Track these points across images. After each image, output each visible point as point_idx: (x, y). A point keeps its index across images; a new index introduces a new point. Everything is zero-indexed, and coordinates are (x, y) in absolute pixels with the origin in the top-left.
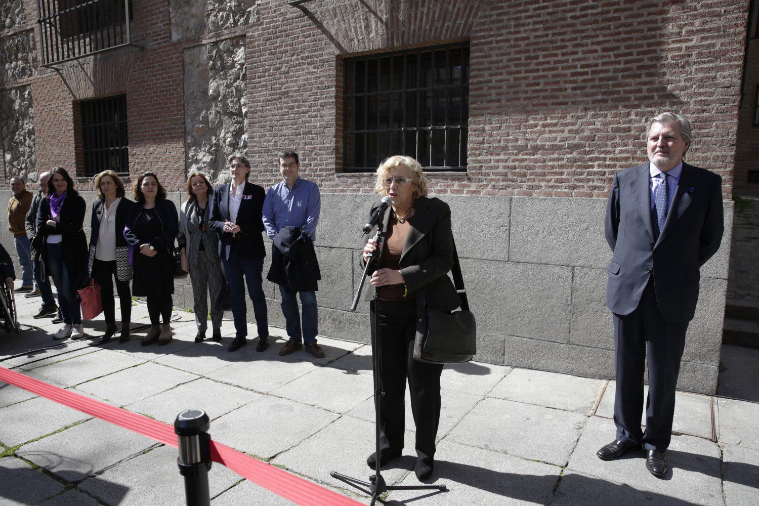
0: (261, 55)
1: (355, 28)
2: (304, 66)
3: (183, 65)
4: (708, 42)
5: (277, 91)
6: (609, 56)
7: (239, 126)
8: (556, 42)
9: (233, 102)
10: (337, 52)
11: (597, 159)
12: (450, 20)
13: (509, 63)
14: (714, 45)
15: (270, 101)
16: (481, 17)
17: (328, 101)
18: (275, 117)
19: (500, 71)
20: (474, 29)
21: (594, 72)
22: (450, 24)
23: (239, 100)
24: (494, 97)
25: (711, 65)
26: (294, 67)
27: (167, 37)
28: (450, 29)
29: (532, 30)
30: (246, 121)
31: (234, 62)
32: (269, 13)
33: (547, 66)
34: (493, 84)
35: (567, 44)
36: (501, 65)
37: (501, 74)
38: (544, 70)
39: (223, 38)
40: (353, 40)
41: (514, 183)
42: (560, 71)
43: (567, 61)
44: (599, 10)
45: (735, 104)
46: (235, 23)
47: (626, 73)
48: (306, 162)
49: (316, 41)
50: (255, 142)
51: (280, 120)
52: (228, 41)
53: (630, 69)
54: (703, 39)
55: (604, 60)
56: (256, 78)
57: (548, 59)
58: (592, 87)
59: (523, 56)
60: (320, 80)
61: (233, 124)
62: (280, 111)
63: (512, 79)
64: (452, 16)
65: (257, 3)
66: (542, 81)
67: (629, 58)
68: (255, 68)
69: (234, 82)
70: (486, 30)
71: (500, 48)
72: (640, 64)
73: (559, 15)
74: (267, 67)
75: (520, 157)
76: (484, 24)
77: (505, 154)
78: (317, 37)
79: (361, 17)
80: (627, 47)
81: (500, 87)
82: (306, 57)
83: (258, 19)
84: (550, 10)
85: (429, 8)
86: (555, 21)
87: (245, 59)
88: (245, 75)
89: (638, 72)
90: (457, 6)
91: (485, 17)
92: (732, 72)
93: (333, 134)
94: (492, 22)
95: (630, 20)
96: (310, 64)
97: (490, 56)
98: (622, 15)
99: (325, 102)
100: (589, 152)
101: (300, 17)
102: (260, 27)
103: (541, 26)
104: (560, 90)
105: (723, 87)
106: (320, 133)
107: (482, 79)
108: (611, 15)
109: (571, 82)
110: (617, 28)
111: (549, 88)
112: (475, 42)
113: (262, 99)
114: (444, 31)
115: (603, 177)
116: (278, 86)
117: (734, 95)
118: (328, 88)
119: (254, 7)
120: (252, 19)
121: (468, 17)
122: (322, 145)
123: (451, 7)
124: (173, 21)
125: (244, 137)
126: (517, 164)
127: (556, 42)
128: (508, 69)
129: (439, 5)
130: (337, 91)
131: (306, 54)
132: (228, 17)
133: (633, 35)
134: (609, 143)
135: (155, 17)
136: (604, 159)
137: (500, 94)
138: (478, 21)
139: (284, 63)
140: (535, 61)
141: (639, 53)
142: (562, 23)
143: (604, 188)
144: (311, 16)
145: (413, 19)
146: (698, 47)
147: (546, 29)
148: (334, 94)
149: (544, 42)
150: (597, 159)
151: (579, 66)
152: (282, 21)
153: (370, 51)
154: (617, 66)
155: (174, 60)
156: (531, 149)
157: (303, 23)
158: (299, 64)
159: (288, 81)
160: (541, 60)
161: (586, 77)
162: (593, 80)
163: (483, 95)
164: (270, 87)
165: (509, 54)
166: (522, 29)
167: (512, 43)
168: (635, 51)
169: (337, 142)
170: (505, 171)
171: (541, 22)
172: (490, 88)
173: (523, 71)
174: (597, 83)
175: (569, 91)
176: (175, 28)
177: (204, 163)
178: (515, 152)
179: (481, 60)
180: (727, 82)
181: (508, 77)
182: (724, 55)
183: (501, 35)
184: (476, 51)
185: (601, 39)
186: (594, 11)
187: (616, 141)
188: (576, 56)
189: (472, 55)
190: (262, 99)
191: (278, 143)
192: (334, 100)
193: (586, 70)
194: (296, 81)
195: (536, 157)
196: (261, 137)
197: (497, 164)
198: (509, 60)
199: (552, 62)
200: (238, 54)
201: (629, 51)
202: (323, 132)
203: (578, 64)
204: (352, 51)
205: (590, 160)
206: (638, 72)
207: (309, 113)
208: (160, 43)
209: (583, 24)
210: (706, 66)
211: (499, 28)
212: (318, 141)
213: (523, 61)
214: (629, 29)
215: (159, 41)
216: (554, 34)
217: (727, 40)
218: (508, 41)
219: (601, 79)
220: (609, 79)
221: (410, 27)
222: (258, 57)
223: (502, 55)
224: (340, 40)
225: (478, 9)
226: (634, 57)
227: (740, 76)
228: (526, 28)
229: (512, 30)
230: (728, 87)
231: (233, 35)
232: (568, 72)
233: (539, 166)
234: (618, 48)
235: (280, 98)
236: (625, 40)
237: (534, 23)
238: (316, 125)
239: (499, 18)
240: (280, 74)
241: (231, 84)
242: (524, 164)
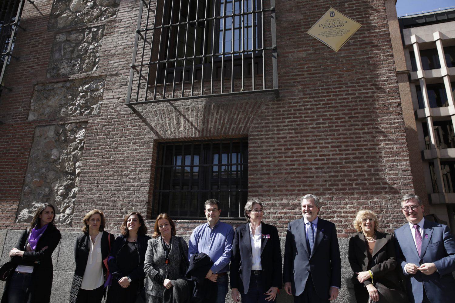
0: (98, 135)
1: (170, 124)
2: (129, 145)
3: (33, 137)
4: (390, 146)
5: (107, 160)
6: (336, 151)
7: (71, 182)
8: (303, 141)
9: (69, 165)
10: (155, 137)
11: (335, 212)
12: (235, 124)
13: (274, 152)
14: (393, 148)
15: (100, 166)
16: (255, 124)
17: (145, 168)
18: (103, 177)
19: (268, 156)
20: (250, 130)
21: (328, 159)
22: (235, 126)
23: (75, 164)
24: (265, 171)
25: (393, 158)
26: (122, 144)
27: (25, 117)
28: (235, 129)
29: (288, 133)
30: (77, 179)
31: (75, 138)
32: (108, 109)
33: (299, 154)
34: (264, 163)
35: (310, 142)
36: (269, 152)
37: (269, 158)
38: (297, 157)
39: (70, 122)
40: (167, 131)
41: (281, 228)
42: (307, 158)
43: (311, 152)
44: (327, 125)
45: (411, 180)
46: (81, 114)
47: (347, 161)
48: (124, 210)
49: (140, 129)
50: (83, 194)
51: (105, 180)
52: (73, 124)
53: (349, 158)
54: (386, 144)
55: (333, 153)
56: (91, 150)
57: (299, 150)
58: (328, 168)
59: (283, 148)
60: (141, 154)
61: (66, 180)
62: (107, 173)
63: (276, 161)
64: (236, 122)
65: (99, 103)
66: (296, 163)
67: (347, 152)
68: (92, 143)
69: (72, 152)
70: (259, 131)
71: (268, 142)
72: (355, 156)
73: (304, 126)
74: (101, 143)
75: (285, 211)
76: (258, 127)
77: (274, 209)
78: (142, 127)
79: (174, 117)
80: (346, 146)
81: (269, 166)
82: (132, 139)
83: (99, 113)
84: (298, 123)
85: (221, 116)
86: (302, 129)
87: (85, 137)
88: (82, 147)
89: (354, 160)
90: (239, 116)
91: (258, 124)
92: (405, 163)
93: (147, 192)
94: (263, 127)
95: (345, 132)
96: (134, 143)
97: (262, 146)
98: (341, 129)
99: (143, 169)
100: (330, 208)
101: (130, 114)
102: (100, 118)
103: (294, 131)
104: (308, 169)
105: (402, 171)
106: (136, 190)
107: (257, 160)
108: (334, 128)
109: (314, 164)
110: (339, 135)
111: (301, 167)
112: (251, 138)
113: (93, 164)
114: (231, 130)
115: (341, 224)
116: (107, 156)
117: (409, 176)
118: (146, 160)
119: (97, 105)
120: (94, 112)
121: (247, 123)
122: (137, 199)
123: (235, 117)
124: (32, 108)
125: (75, 190)
126: (282, 215)
127: (303, 141)
128: (274, 155)
129: (227, 115)
130: (152, 163)
131: (132, 137)
132: (76, 110)
133: (348, 140)
134: (342, 202)
135: (18, 104)
136: (340, 212)
137: (270, 170)
138: (254, 126)
139: (115, 141)
140: (291, 151)
141: (353, 150)
142: (306, 130)
143: (342, 231)
144: (138, 114)
145: (210, 121)
146: (385, 148)
147: (296, 133)
148: (150, 164)
149: (296, 141)
150: (335, 212)
151: (318, 155)
152: (117, 115)
153: (179, 139)
154: (341, 157)
155: (27, 133)
156: (291, 206)
157: (132, 118)
158: (126, 143)
159: (115, 154)
160: (294, 150)
161: (323, 162)
162: (328, 164)
163: (258, 170)
164: (101, 156)
165: (274, 146)
166: (282, 132)
167: (276, 140)
168: (350, 148)
169: (149, 197)
170: (275, 220)
171: (293, 129)
172: (262, 166)
173: (284, 156)
174: (330, 165)
175: (314, 170)
176: (33, 112)
177: (35, 208)
178: (281, 207)
179: (255, 149)
180: (404, 168)
181: (274, 160)
182: (399, 154)
183: (269, 135)
184: (253, 143)
185: (330, 141)
186: (324, 125)
187: (346, 201)
188: (316, 150)
189: (249, 145)
190: (93, 164)
191: (102, 196)
192: (150, 168)
193: (323, 157)
194: (122, 154)
195: (295, 211)
196: (88, 191)
197: (268, 215)
198: (274, 150)
199: (302, 152)
200: (79, 133)
201: (347, 148)
202: (140, 190)
203: (318, 154)
204: (166, 138)
205: (331, 213)
206: (354, 160)
207: (130, 176)
208: (18, 121)
209: (318, 132)
210: (391, 159)
211: (267, 131)
212: (134, 196)
213: (283, 151)
214: (345, 136)
215: (17, 119)
216: (301, 136)
217: (399, 146)
218: (273, 138)
219: (333, 163)
220: (338, 163)
221: (208, 126)
222: (95, 136)
223: (270, 146)
224: (158, 129)
225: (253, 119)
226: (350, 152)
227: (410, 165)
228: (284, 132)
229: (275, 132)
230: (405, 171)
231: (78, 121)
232: (313, 158)
233: (298, 217)
234: (341, 146)
235: (108, 165)
236: (344, 142)
237: (289, 129)
238: (135, 185)
239: (266, 125)
240: (110, 148)
241: (70, 153)
242: (287, 215)
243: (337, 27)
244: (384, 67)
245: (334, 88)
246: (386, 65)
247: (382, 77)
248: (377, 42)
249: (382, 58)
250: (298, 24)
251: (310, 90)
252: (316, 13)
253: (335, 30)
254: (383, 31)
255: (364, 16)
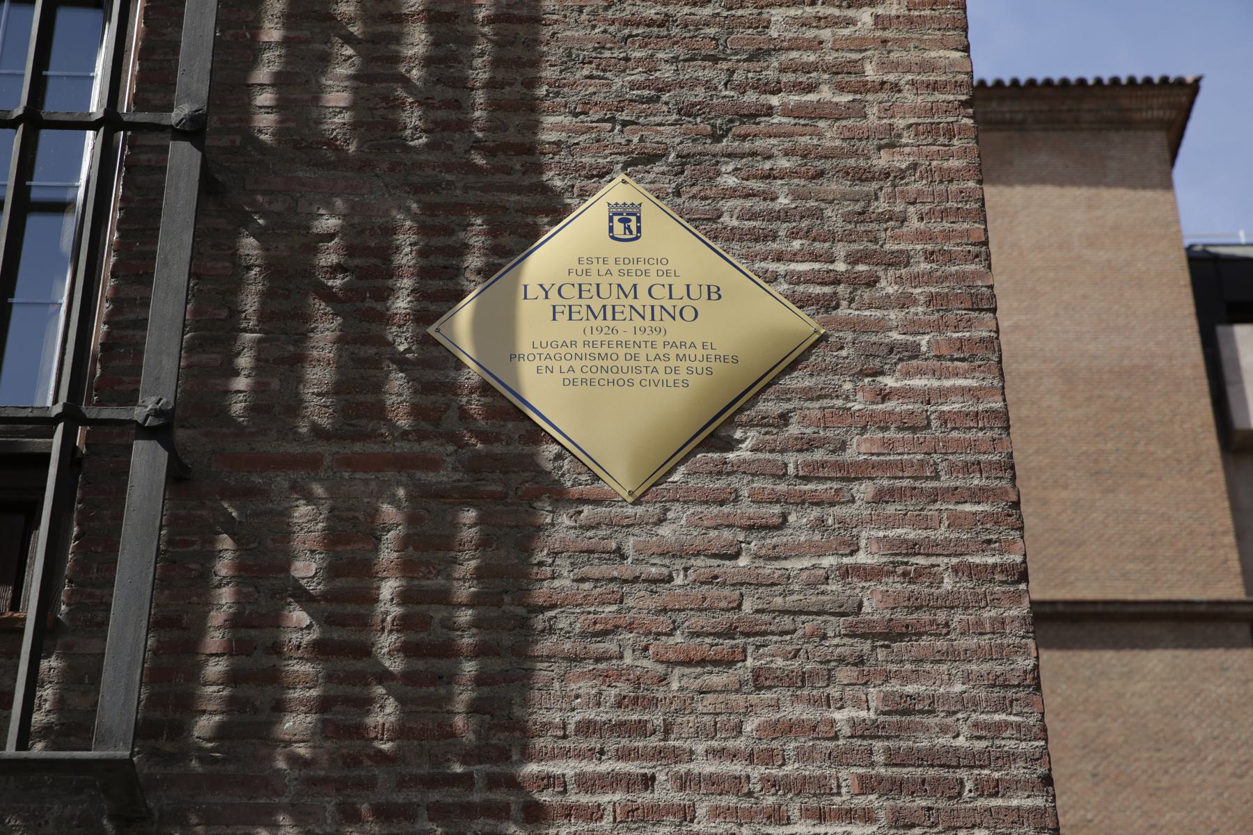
243: (647, 323)
244: (952, 656)
245: (587, 783)
246: (972, 642)
247: (944, 730)
248: (922, 464)
249: (948, 583)
250: (372, 261)
251: (402, 784)
252: (514, 198)
253: (630, 337)
254: (964, 391)
255: (841, 267)
